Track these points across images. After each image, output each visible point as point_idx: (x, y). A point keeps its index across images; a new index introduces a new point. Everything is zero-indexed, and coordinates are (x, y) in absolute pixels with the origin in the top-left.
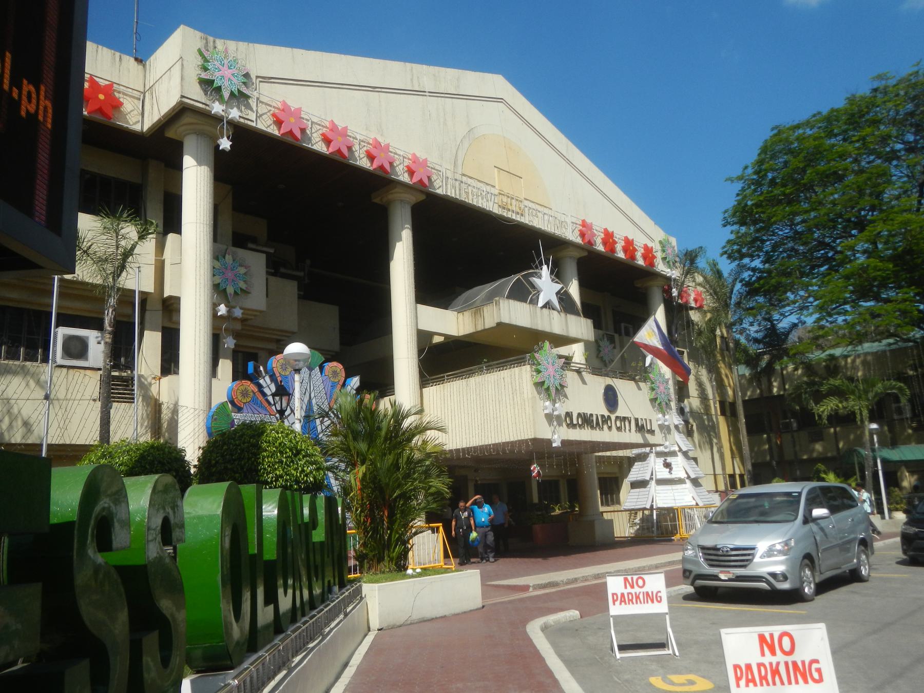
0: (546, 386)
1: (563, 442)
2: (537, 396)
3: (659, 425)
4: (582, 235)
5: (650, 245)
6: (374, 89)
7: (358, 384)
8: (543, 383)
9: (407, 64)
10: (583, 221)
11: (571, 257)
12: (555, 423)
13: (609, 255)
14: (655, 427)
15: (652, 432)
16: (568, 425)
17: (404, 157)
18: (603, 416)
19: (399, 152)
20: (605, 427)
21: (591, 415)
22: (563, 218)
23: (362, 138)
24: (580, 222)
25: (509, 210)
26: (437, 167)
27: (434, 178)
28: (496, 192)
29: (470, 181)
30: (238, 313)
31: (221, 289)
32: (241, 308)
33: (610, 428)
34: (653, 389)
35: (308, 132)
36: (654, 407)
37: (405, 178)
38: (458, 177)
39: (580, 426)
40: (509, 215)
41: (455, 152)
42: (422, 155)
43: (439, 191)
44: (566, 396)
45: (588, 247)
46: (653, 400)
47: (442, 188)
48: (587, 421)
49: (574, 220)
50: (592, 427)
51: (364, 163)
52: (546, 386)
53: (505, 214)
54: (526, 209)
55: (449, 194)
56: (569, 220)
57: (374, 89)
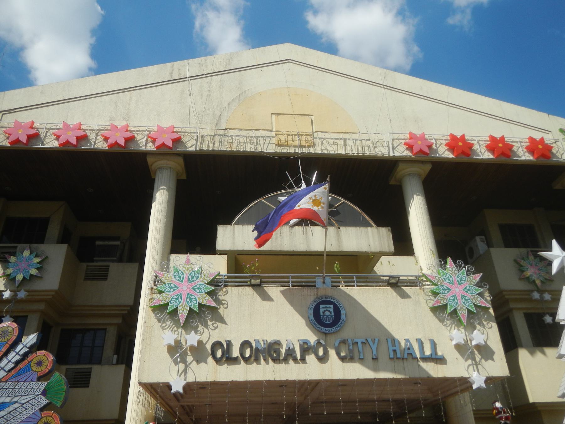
0: (170, 309)
1: (188, 387)
2: (157, 325)
3: (458, 347)
4: (410, 147)
5: (537, 136)
6: (125, 90)
7: (35, 340)
8: (166, 305)
9: (169, 65)
10: (410, 134)
11: (409, 175)
12: (190, 358)
13: (464, 159)
14: (446, 349)
15: (440, 360)
16: (218, 361)
17: (150, 132)
18: (305, 342)
19: (141, 129)
20: (311, 358)
21: (278, 343)
22: (374, 138)
23: (99, 127)
24: (408, 136)
25: (289, 146)
26: (188, 130)
27: (185, 139)
28: (273, 134)
29: (231, 133)
30: (22, 294)
31: (11, 277)
32: (25, 291)
33: (323, 359)
34: (435, 294)
35: (42, 136)
36: (442, 321)
37: (151, 147)
38: (221, 132)
39: (246, 360)
40: (292, 150)
41: (218, 114)
42: (166, 124)
43: (193, 149)
44: (222, 320)
45: (422, 157)
46: (439, 310)
47: (191, 146)
48: (272, 352)
49: (396, 136)
50: (276, 360)
51: (102, 145)
52: (170, 309)
53: (285, 151)
54: (318, 142)
55: (205, 148)
56: (387, 138)
57: (125, 90)
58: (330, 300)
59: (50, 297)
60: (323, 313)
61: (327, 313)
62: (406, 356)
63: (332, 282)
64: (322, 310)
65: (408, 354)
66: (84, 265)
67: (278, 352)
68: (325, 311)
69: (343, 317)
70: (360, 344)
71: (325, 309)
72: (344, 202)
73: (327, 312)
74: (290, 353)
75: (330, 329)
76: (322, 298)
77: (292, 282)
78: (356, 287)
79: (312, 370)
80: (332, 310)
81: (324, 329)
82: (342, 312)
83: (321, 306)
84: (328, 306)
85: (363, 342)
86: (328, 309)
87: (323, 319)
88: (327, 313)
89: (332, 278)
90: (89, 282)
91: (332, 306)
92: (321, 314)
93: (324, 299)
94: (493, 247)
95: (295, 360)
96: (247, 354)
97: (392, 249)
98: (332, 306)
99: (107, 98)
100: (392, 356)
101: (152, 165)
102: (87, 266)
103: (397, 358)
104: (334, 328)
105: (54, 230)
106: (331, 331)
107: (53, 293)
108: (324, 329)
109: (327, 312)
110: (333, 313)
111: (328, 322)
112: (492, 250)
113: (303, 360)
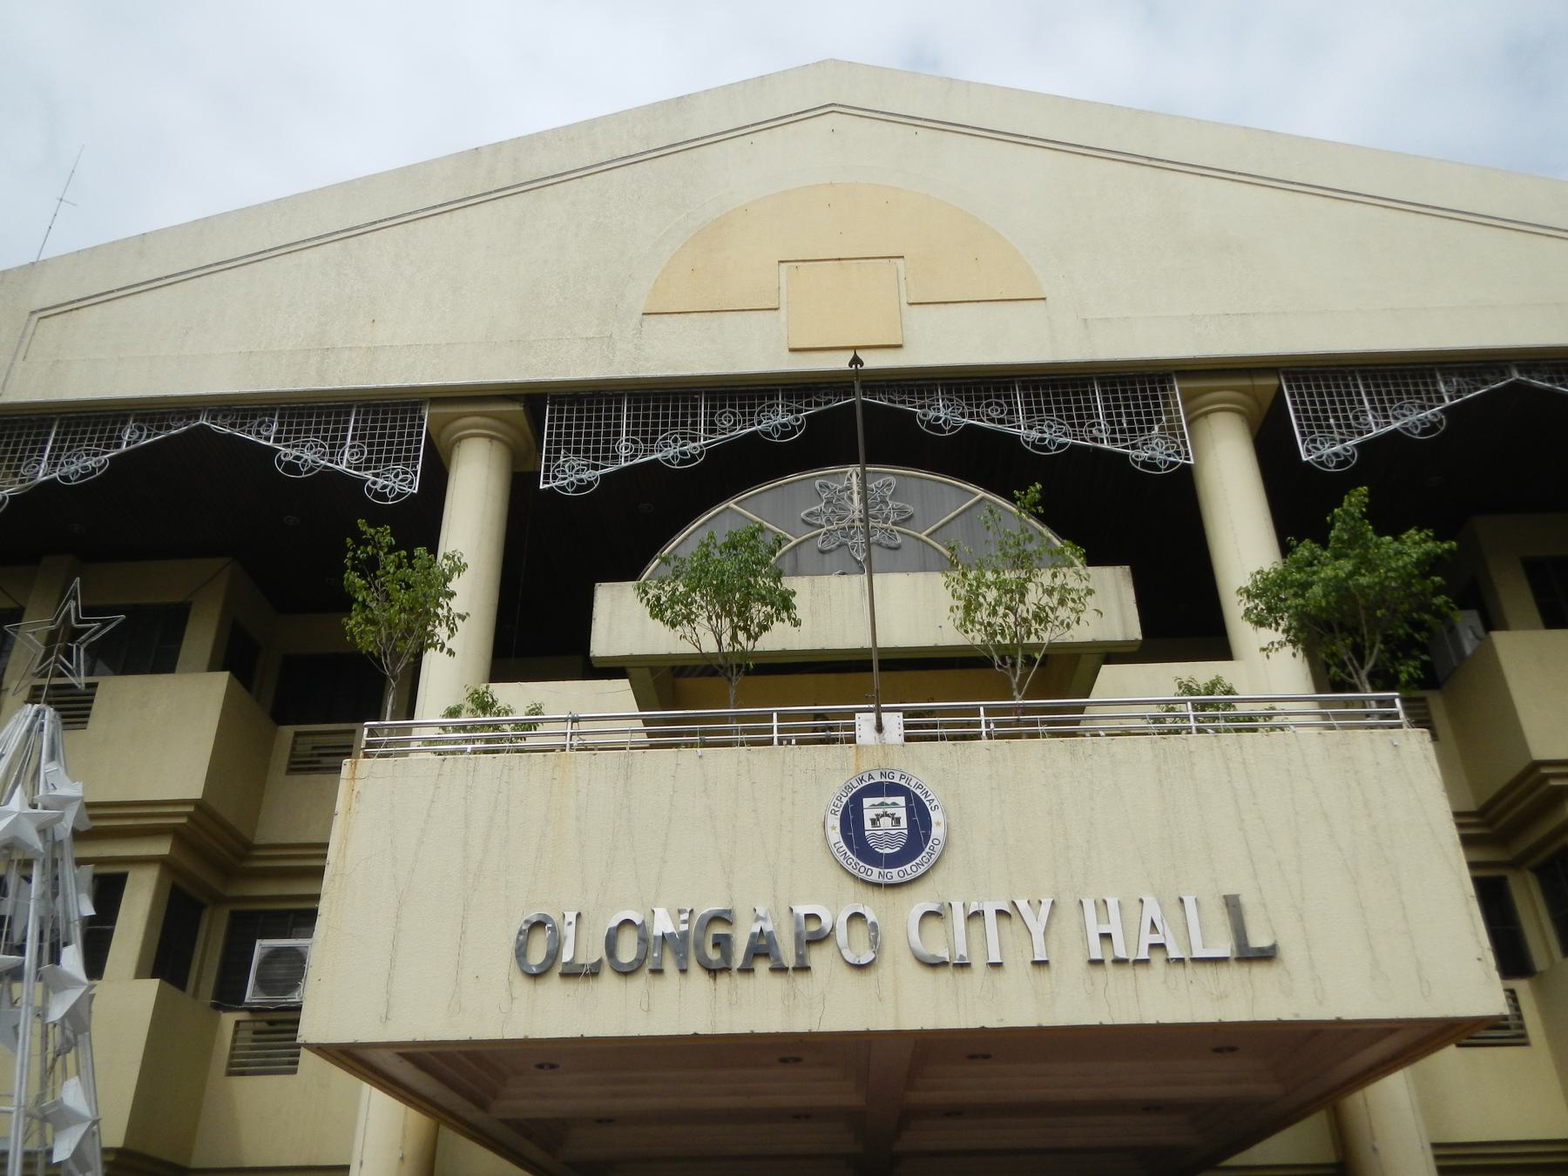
39: (626, 972)
58: (896, 780)
59: (184, 820)
60: (874, 822)
61: (886, 823)
62: (1144, 955)
63: (907, 726)
64: (869, 815)
65: (1152, 946)
66: (288, 731)
67: (723, 943)
68: (879, 817)
69: (937, 832)
70: (990, 916)
71: (880, 811)
72: (982, 499)
73: (885, 821)
74: (762, 948)
75: (894, 871)
76: (870, 777)
77: (780, 730)
78: (985, 742)
79: (830, 1004)
80: (901, 813)
81: (875, 874)
82: (935, 816)
83: (867, 802)
84: (889, 800)
85: (1000, 913)
86: (890, 811)
87: (871, 843)
88: (886, 823)
89: (908, 714)
90: (298, 778)
91: (901, 800)
92: (868, 825)
93: (878, 779)
94: (1504, 626)
95: (779, 969)
96: (628, 951)
97: (1136, 633)
98: (901, 800)
99: (313, 255)
100: (1097, 955)
101: (439, 436)
102: (297, 734)
103: (1119, 962)
104: (907, 867)
105: (200, 637)
106: (896, 879)
107: (190, 809)
108: (876, 870)
109: (885, 821)
110: (904, 823)
111: (888, 851)
112: (1498, 637)
113: (803, 968)
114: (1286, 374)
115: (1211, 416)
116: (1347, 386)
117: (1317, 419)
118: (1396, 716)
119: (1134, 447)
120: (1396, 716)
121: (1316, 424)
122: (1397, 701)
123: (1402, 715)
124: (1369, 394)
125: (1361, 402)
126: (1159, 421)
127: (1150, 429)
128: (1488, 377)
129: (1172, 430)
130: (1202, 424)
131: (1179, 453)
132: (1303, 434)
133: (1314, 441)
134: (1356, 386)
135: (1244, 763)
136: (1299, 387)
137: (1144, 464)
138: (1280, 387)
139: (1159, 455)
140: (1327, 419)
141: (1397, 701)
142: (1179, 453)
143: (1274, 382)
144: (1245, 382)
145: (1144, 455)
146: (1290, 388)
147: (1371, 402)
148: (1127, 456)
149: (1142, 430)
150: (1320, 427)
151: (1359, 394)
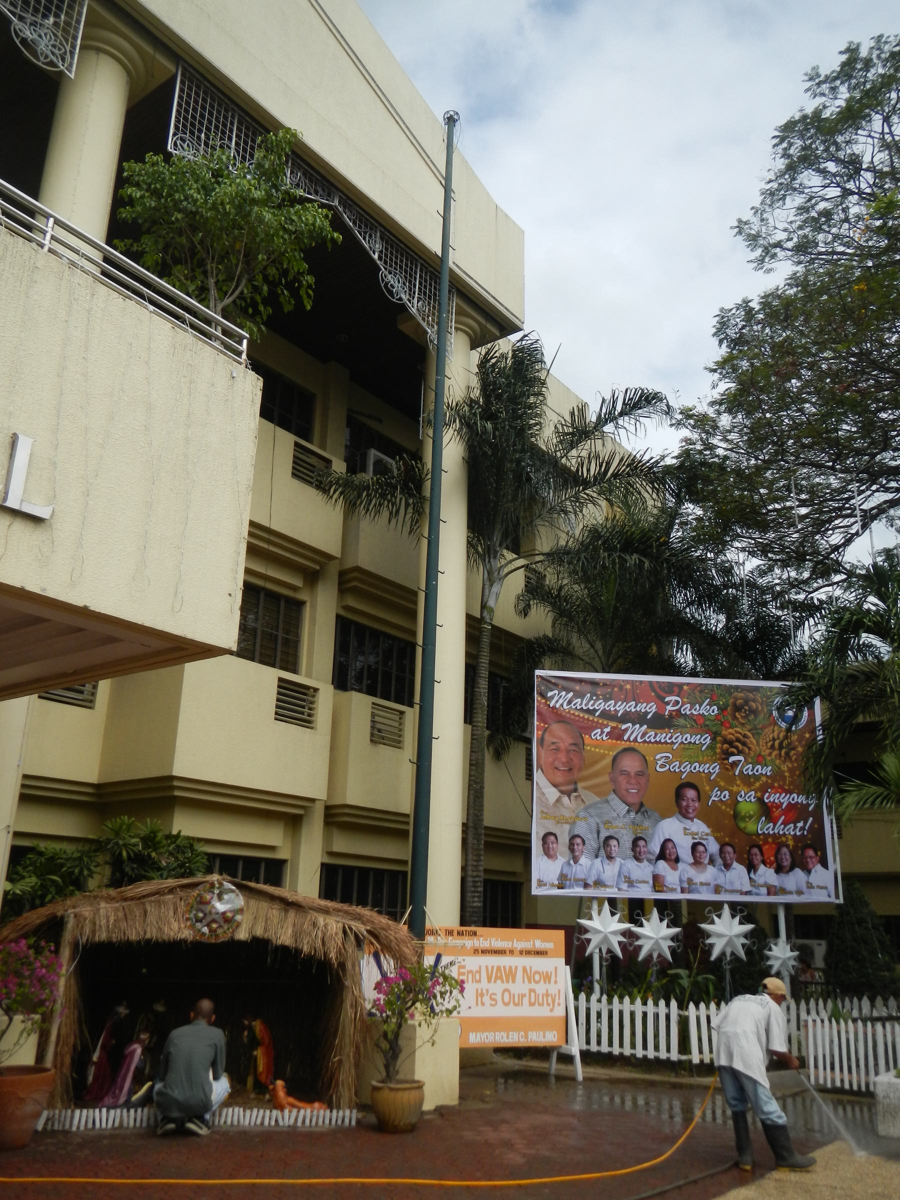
114: (184, 69)
115: (103, 56)
116: (226, 118)
117: (193, 125)
118: (239, 354)
119: (21, 19)
120: (239, 354)
121: (189, 127)
122: (245, 342)
123: (244, 356)
124: (238, 136)
125: (230, 139)
126: (57, 16)
127: (45, 16)
128: (321, 192)
129: (67, 31)
130: (92, 55)
131: (63, 60)
132: (177, 128)
133: (183, 140)
134: (232, 123)
135: (89, 311)
136: (190, 88)
137: (24, 41)
138: (174, 78)
139: (44, 45)
140: (200, 131)
141: (245, 342)
142: (63, 60)
143: (171, 67)
144: (149, 49)
145: (28, 34)
146: (182, 82)
147: (237, 144)
148: (10, 22)
149: (36, 10)
150: (192, 133)
151: (231, 131)
